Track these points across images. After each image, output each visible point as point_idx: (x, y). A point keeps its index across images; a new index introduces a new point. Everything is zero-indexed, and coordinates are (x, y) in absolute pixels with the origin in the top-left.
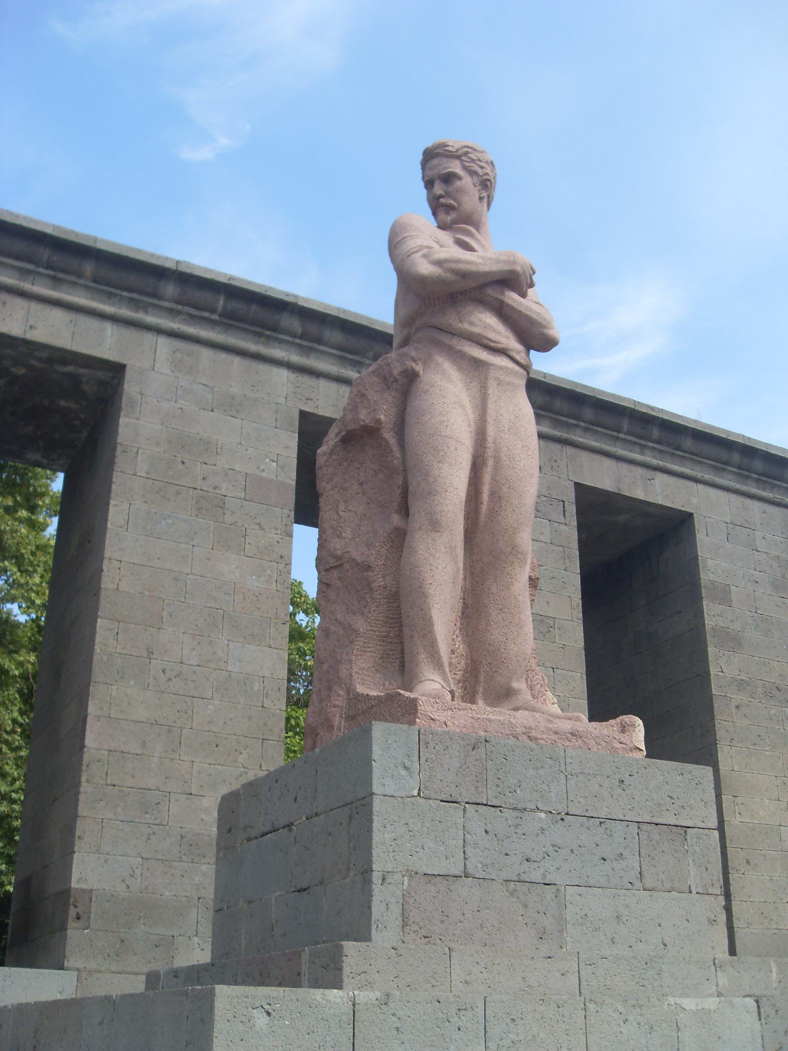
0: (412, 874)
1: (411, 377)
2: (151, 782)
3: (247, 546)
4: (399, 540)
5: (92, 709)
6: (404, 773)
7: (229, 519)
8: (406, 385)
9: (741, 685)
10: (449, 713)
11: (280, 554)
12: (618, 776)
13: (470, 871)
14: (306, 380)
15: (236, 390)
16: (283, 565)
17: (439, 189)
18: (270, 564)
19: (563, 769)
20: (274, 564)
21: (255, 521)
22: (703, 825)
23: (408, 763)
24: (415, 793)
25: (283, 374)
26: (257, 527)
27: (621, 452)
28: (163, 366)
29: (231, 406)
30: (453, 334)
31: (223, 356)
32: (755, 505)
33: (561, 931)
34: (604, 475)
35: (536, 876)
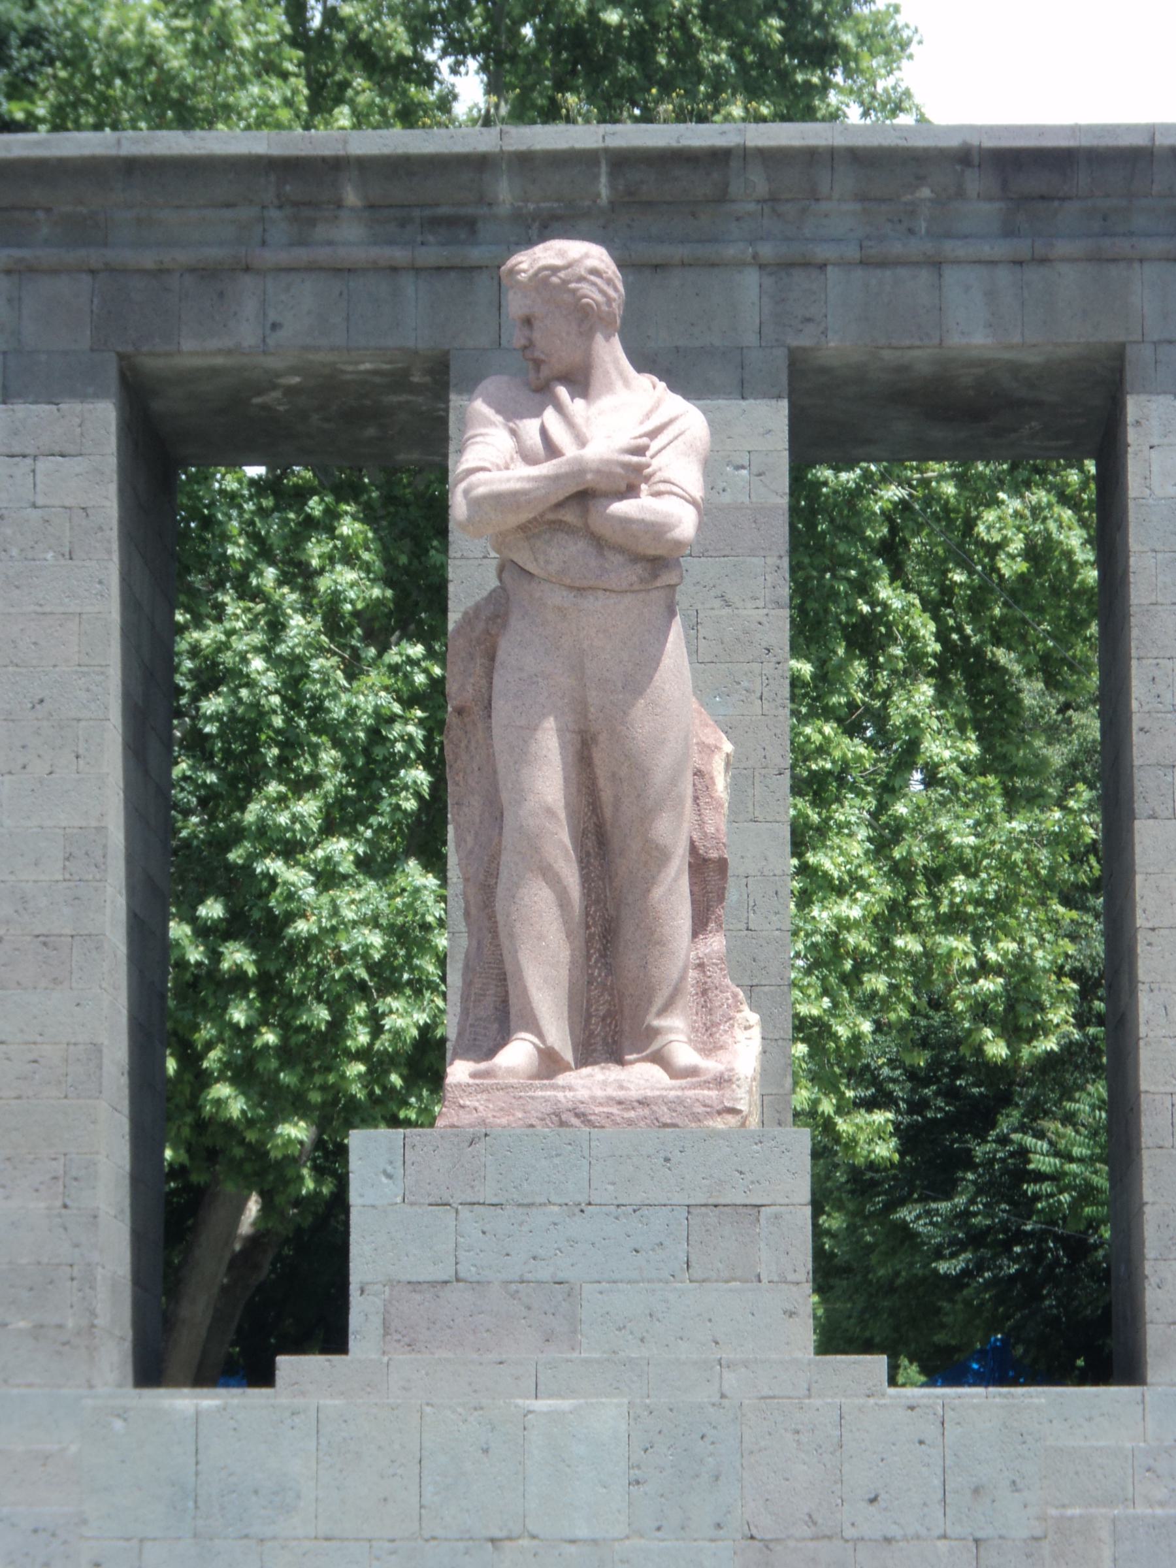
0: (392, 1283)
3: (702, 642)
6: (384, 1180)
10: (485, 1096)
11: (764, 644)
12: (662, 1154)
13: (462, 1275)
16: (772, 665)
18: (746, 667)
19: (586, 1153)
20: (756, 667)
21: (713, 593)
22: (786, 1201)
23: (389, 1169)
24: (399, 1199)
26: (718, 603)
33: (574, 1332)
35: (544, 1273)
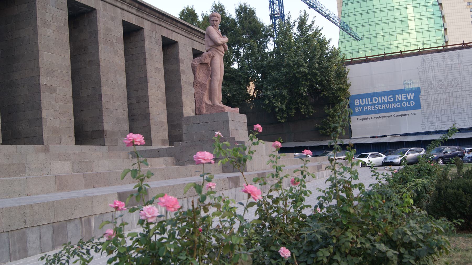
1: (214, 56)
2: (111, 107)
4: (211, 81)
5: (102, 93)
7: (115, 48)
8: (212, 58)
9: (185, 82)
14: (122, 11)
15: (112, 15)
17: (215, 22)
25: (119, 9)
27: (169, 28)
28: (102, 10)
29: (113, 19)
30: (219, 50)
31: (110, 6)
32: (187, 39)
34: (166, 33)
